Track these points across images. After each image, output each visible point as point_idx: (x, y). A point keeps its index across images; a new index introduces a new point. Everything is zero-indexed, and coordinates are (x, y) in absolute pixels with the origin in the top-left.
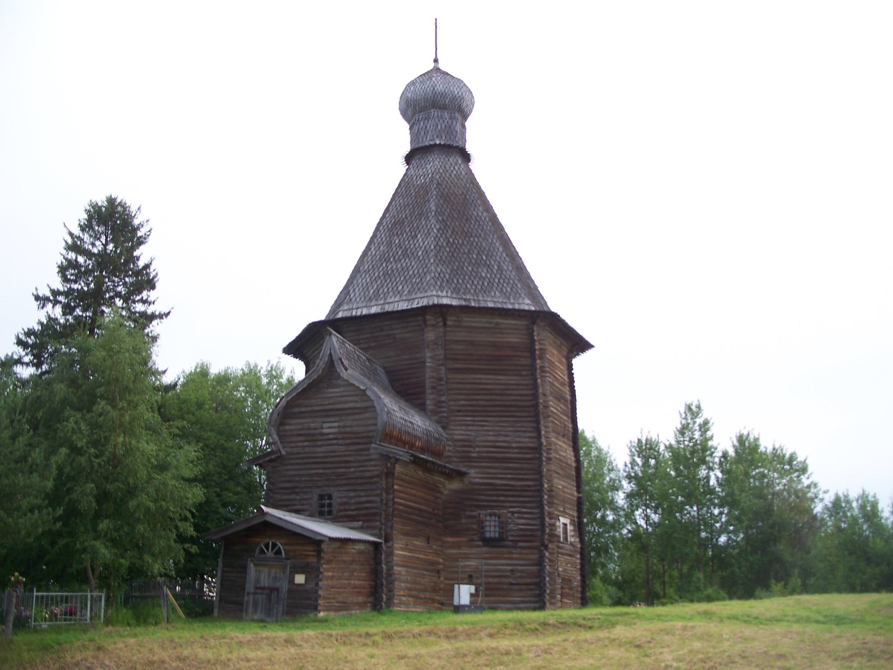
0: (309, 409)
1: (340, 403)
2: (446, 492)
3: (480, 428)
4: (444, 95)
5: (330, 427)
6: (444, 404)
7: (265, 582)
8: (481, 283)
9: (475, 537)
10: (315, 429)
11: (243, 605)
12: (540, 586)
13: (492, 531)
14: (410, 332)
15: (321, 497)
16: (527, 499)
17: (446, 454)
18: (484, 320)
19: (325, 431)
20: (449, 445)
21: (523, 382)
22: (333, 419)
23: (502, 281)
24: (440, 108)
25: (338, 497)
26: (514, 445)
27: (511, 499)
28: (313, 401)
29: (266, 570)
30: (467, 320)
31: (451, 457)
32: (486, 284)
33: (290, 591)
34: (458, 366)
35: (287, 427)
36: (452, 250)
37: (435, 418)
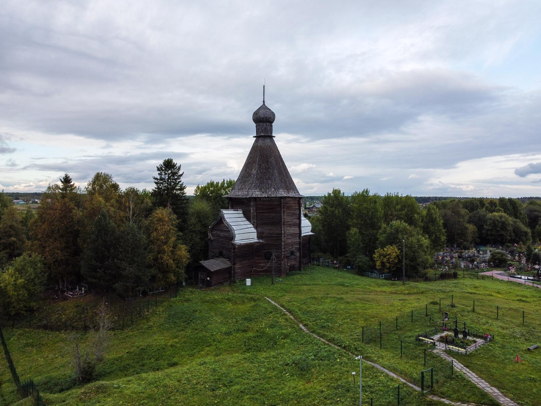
4: (263, 118)
5: (222, 234)
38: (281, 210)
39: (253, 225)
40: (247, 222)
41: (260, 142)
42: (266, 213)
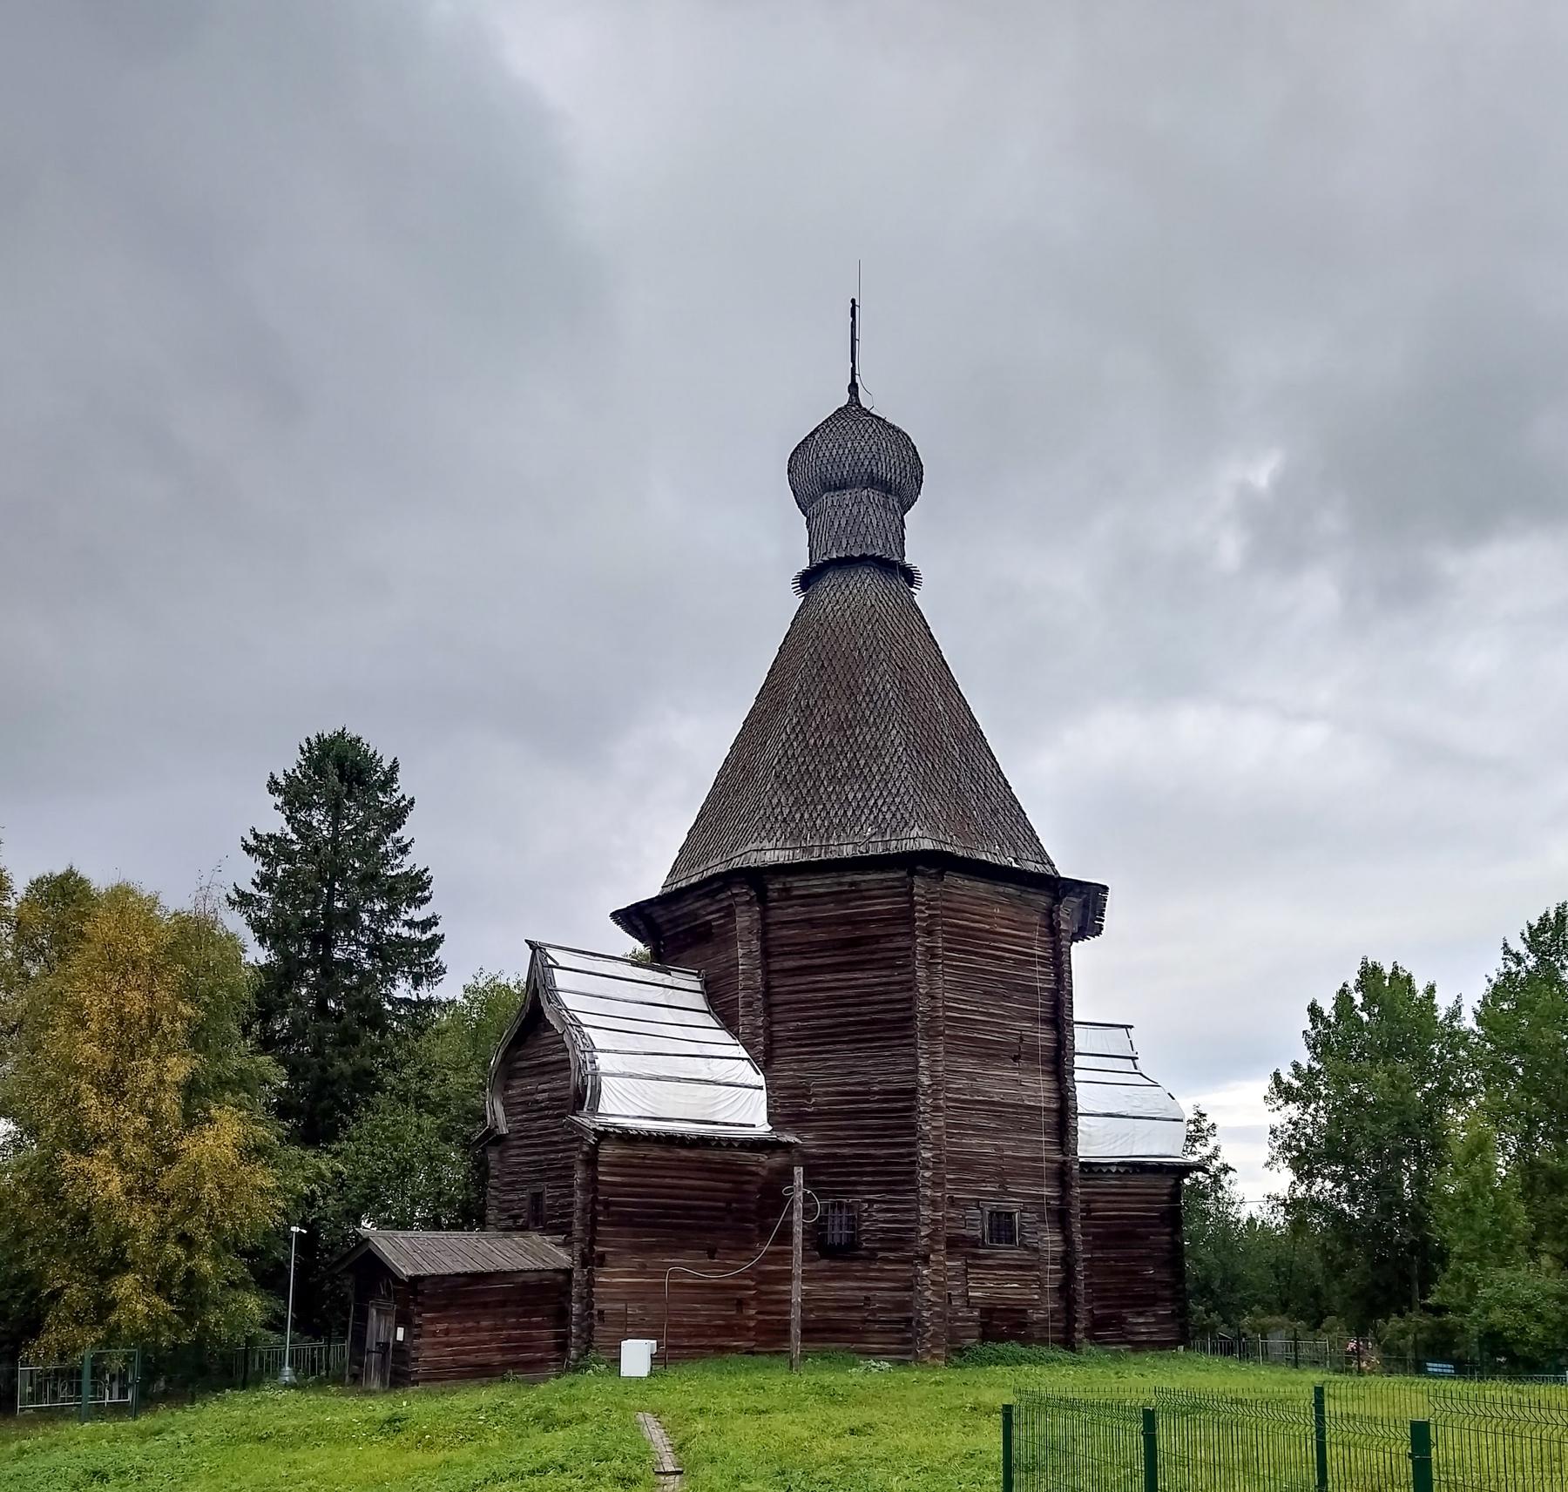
19: (539, 1097)
22: (545, 1078)
23: (880, 802)
24: (837, 488)
30: (799, 884)
32: (849, 813)
39: (747, 1046)
40: (723, 1036)
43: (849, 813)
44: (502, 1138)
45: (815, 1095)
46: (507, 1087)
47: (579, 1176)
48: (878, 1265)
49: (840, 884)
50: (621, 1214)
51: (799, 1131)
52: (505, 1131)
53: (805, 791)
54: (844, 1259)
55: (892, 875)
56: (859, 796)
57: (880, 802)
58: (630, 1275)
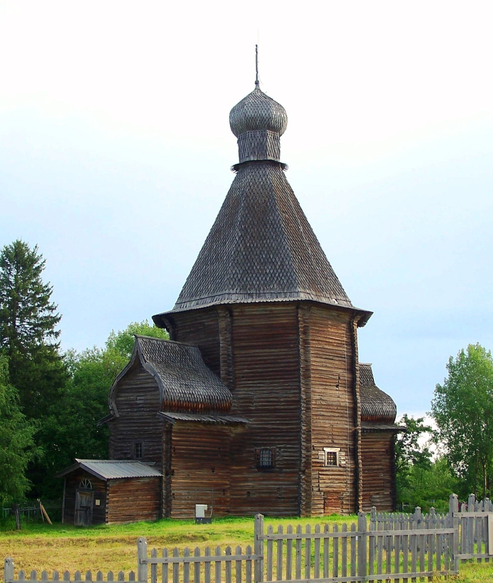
0: (130, 387)
1: (145, 383)
2: (232, 435)
3: (258, 389)
6: (231, 374)
7: (84, 504)
8: (264, 279)
9: (253, 466)
10: (133, 400)
11: (74, 516)
12: (298, 499)
13: (265, 460)
14: (211, 321)
15: (137, 445)
16: (292, 438)
17: (233, 408)
18: (261, 309)
19: (138, 402)
20: (235, 402)
21: (291, 353)
22: (142, 394)
23: (281, 275)
25: (145, 445)
26: (282, 400)
27: (279, 438)
28: (132, 381)
29: (84, 496)
31: (235, 410)
32: (268, 279)
33: (94, 510)
34: (244, 344)
35: (120, 399)
36: (247, 253)
37: (226, 383)
38: (297, 340)
41: (249, 175)
42: (256, 347)
43: (268, 279)
44: (116, 418)
45: (255, 402)
46: (118, 396)
47: (164, 438)
48: (283, 475)
49: (266, 311)
50: (180, 453)
51: (248, 417)
52: (118, 416)
53: (247, 268)
54: (268, 472)
55: (288, 308)
56: (272, 271)
57: (281, 275)
58: (183, 479)
